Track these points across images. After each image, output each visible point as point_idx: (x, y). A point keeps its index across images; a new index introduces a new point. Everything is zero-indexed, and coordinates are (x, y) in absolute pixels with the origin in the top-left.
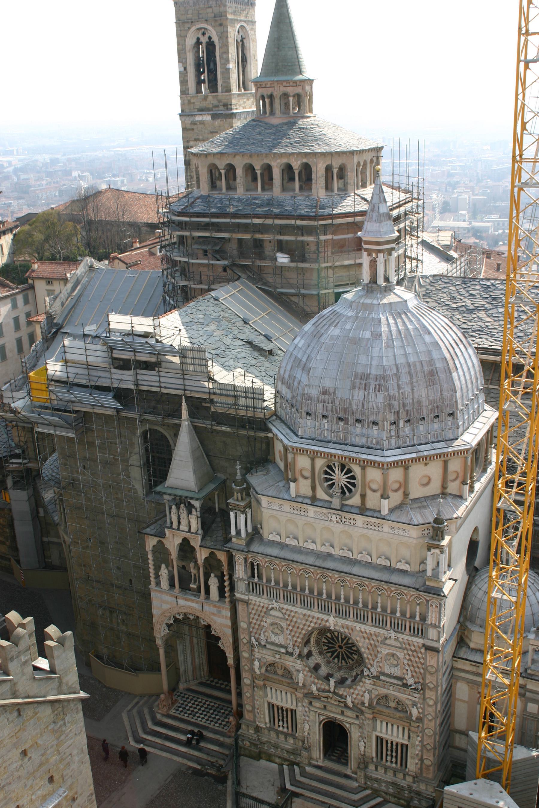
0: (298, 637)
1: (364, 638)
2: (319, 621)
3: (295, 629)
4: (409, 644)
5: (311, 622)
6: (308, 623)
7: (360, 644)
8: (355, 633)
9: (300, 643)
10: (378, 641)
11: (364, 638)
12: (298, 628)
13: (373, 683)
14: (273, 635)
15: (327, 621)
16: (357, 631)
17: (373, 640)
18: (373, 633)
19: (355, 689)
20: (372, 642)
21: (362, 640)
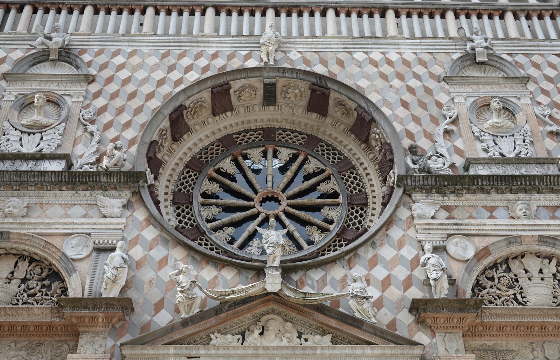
0: (127, 125)
1: (384, 77)
2: (219, 62)
3: (118, 102)
4: (537, 66)
5: (188, 69)
6: (175, 75)
7: (374, 97)
8: (353, 69)
9: (132, 142)
10: (432, 76)
11: (384, 77)
12: (132, 96)
13: (444, 214)
14: (14, 135)
15: (247, 57)
16: (359, 64)
17: (418, 77)
18: (409, 56)
19: (373, 263)
20: (414, 83)
21: (380, 83)
